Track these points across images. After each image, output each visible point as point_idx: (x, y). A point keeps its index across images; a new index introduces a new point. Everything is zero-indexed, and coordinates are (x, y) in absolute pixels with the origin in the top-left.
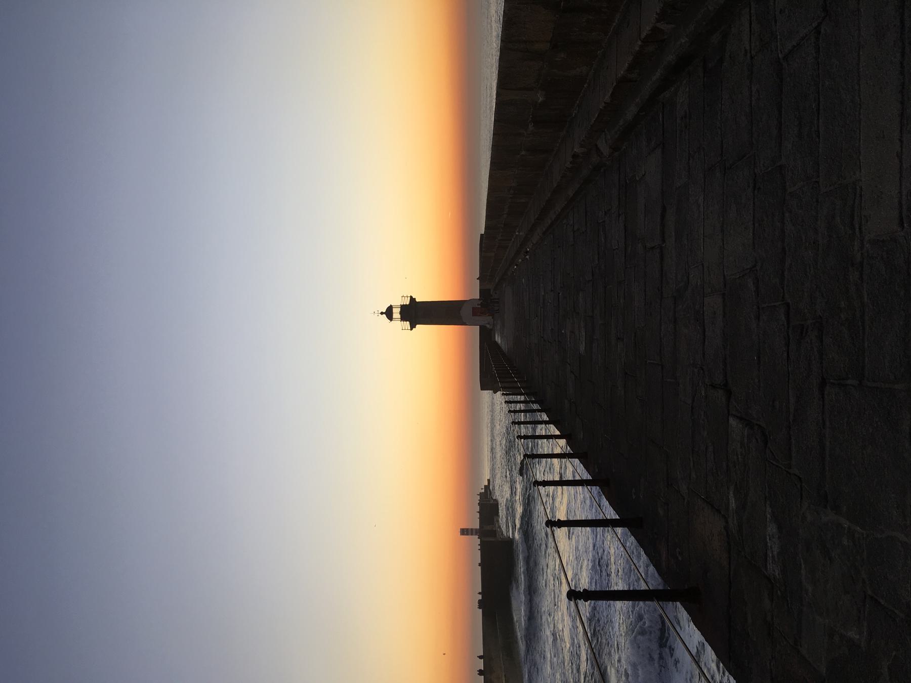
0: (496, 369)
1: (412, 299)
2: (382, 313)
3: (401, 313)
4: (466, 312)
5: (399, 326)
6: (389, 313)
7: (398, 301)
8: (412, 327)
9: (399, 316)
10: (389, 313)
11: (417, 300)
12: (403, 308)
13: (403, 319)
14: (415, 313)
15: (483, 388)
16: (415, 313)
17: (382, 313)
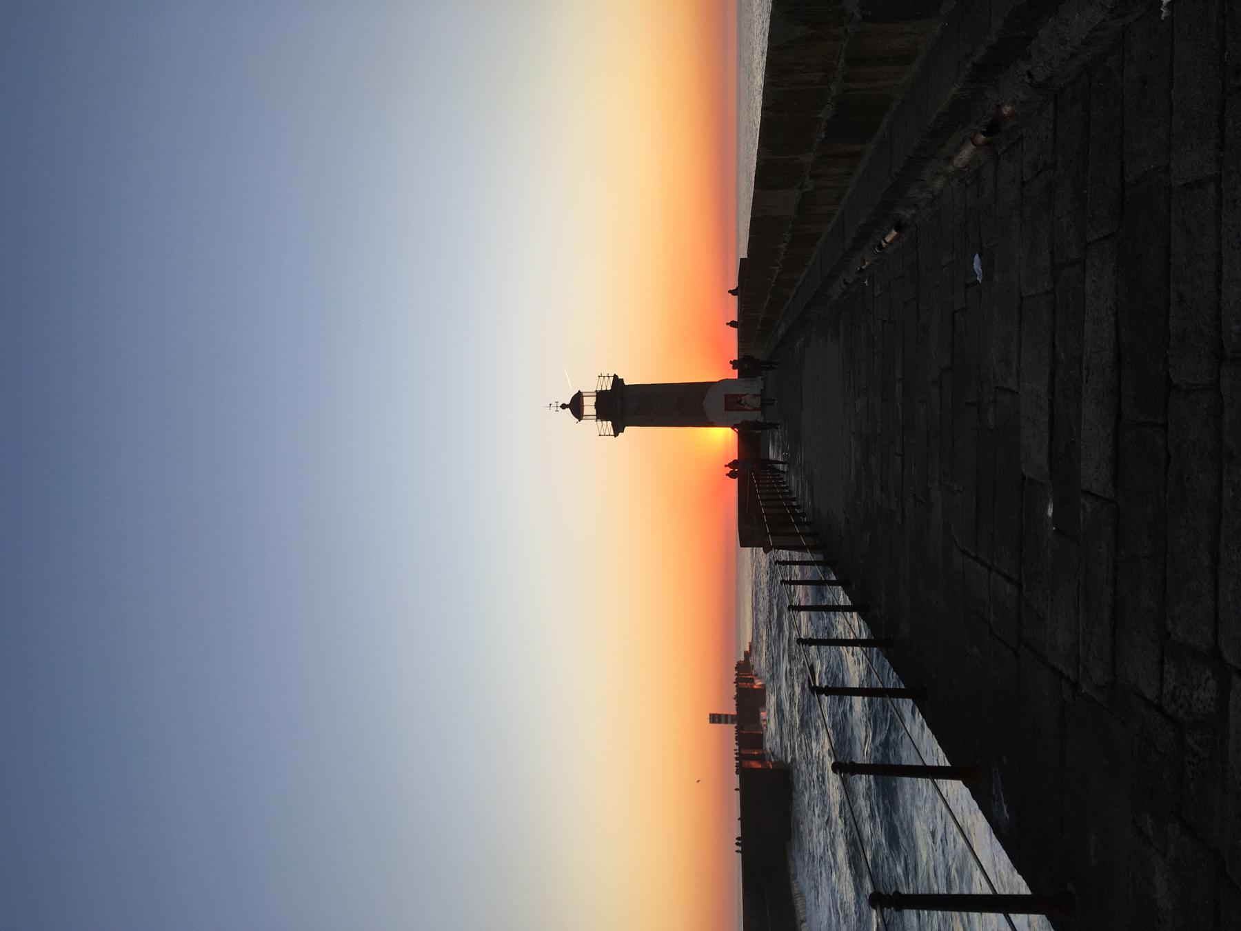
0: (764, 508)
1: (617, 381)
2: (564, 406)
3: (597, 406)
4: (713, 403)
5: (594, 429)
6: (576, 406)
7: (593, 383)
8: (617, 430)
9: (594, 412)
10: (576, 406)
11: (626, 383)
12: (600, 395)
13: (601, 415)
14: (623, 405)
15: (744, 543)
16: (623, 405)
17: (564, 406)
